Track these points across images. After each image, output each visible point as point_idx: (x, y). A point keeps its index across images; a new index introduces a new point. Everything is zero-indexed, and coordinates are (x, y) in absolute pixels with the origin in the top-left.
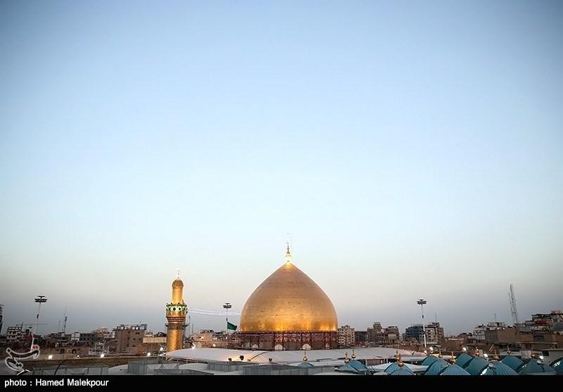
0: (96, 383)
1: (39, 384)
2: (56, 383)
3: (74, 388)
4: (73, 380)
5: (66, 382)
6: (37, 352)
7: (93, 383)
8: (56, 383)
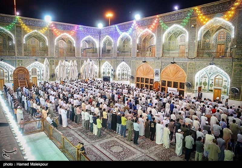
0: (42, 164)
1: (18, 165)
2: (26, 164)
3: (33, 166)
4: (33, 163)
5: (30, 164)
6: (16, 151)
7: (41, 165)
8: (26, 164)
